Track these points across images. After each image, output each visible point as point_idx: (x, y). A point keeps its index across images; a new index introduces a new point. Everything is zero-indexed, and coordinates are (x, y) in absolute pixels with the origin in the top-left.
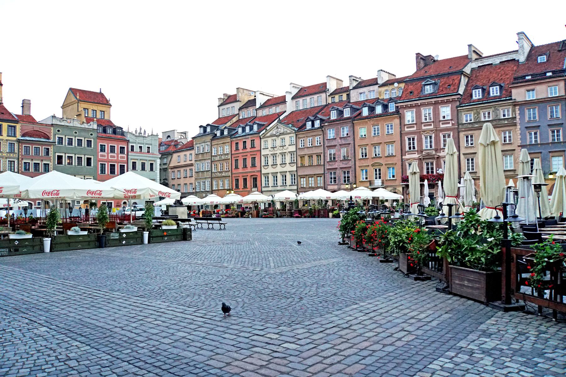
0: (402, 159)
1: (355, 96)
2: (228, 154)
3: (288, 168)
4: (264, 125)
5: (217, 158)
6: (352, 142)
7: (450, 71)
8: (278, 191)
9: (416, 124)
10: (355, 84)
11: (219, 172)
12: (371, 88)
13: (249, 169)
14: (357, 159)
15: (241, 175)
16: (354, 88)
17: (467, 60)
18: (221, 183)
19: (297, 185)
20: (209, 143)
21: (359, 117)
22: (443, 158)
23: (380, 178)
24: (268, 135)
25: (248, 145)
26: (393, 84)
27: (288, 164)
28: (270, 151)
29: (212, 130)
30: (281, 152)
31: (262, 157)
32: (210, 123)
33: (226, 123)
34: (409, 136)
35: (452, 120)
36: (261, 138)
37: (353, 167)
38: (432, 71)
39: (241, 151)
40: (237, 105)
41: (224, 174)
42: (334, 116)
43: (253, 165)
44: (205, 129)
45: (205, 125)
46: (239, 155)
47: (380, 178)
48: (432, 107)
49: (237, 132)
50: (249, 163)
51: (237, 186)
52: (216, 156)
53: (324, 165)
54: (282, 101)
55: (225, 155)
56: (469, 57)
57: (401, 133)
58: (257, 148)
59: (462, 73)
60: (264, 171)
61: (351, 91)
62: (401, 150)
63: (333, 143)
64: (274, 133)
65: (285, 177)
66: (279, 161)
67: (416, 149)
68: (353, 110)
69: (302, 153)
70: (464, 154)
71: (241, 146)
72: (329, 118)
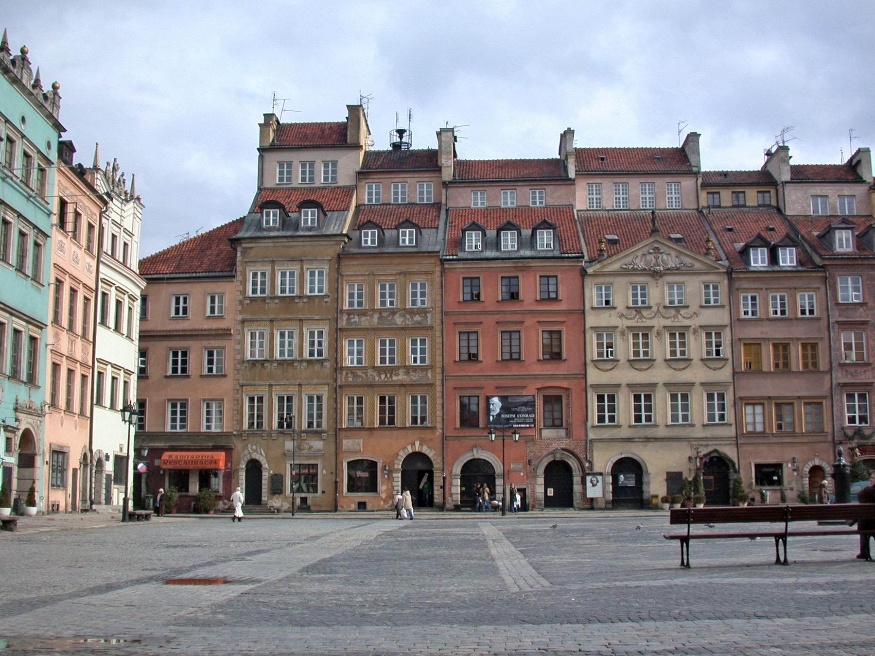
1: (799, 202)
2: (423, 312)
3: (697, 374)
5: (364, 322)
8: (656, 439)
28: (622, 316)
30: (668, 323)
41: (401, 377)
46: (482, 318)
52: (363, 313)
55: (412, 312)
60: (594, 376)
63: (859, 315)
64: (641, 265)
66: (661, 348)
69: (753, 332)
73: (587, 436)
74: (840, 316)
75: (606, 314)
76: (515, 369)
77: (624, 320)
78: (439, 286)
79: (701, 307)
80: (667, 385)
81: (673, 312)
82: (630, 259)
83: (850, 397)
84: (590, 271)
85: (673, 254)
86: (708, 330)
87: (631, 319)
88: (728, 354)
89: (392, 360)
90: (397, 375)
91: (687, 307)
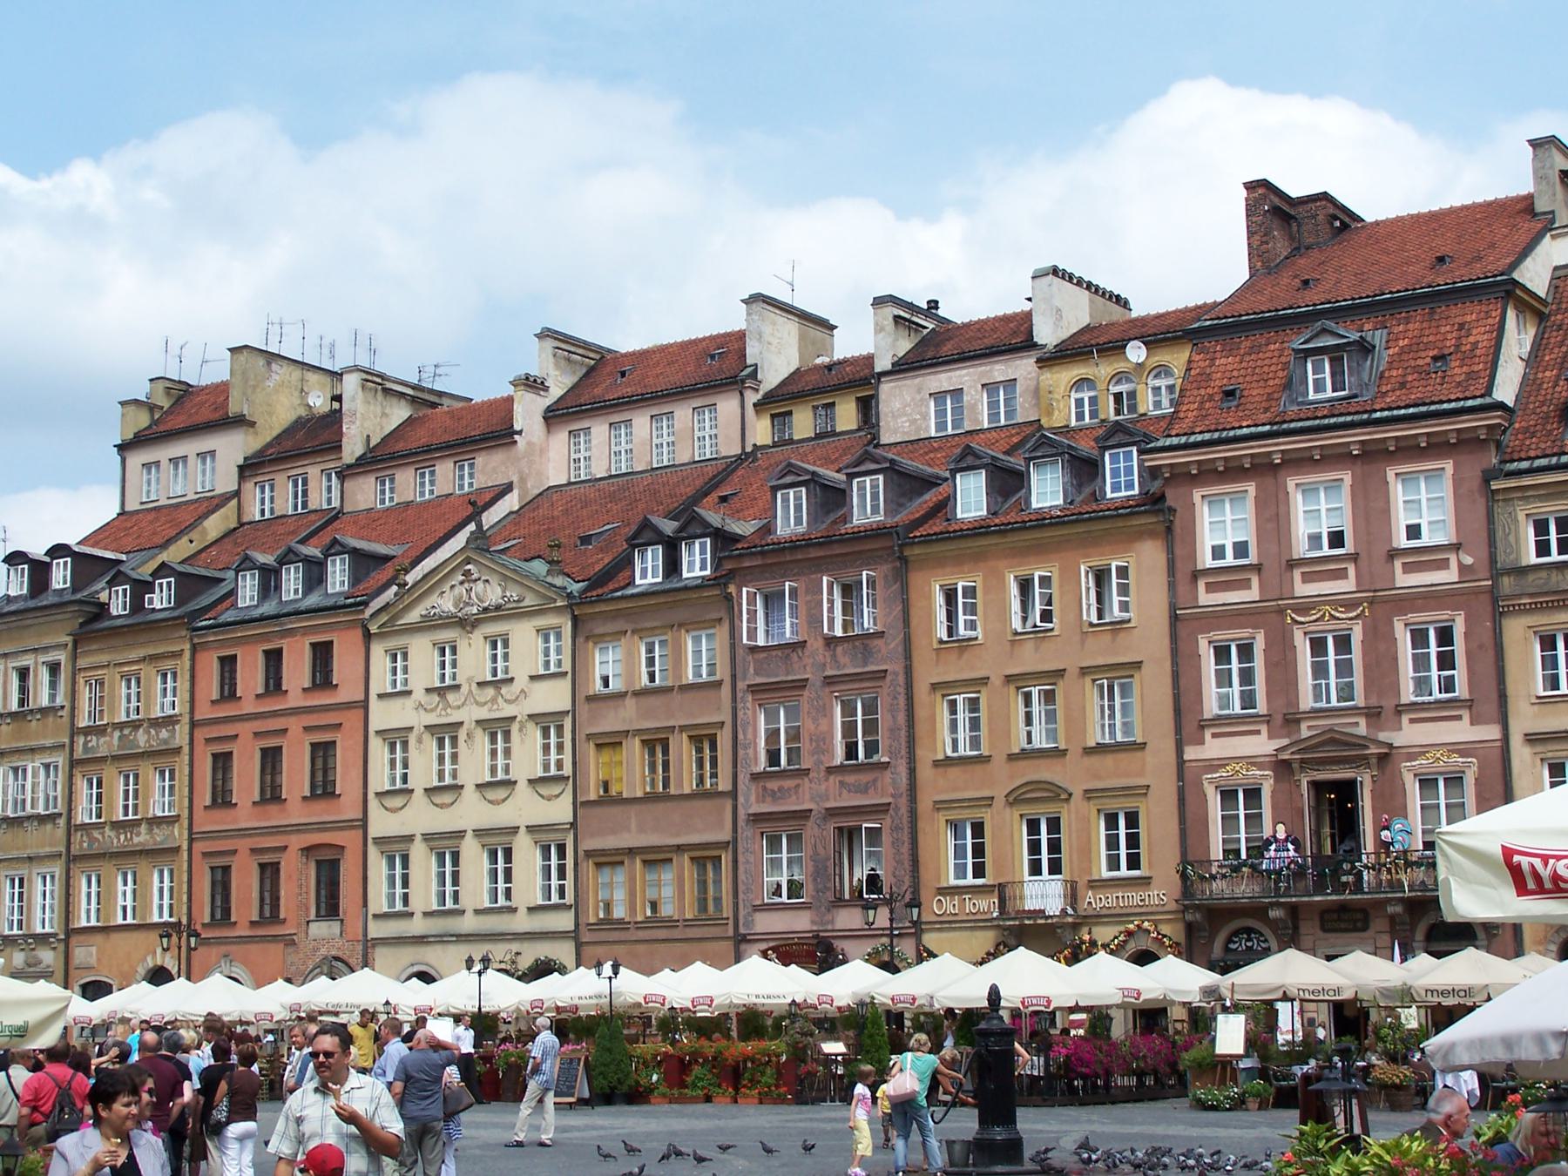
0: (1181, 763)
1: (908, 412)
2: (170, 721)
3: (525, 808)
4: (387, 559)
5: (106, 745)
6: (895, 667)
7: (1443, 279)
9: (1257, 568)
10: (905, 345)
11: (117, 825)
12: (999, 370)
13: (295, 811)
14: (924, 756)
15: (243, 845)
16: (904, 367)
17: (1528, 227)
18: (124, 893)
19: (577, 907)
20: (62, 656)
21: (937, 526)
22: (1412, 757)
23: (1055, 868)
24: (414, 616)
25: (297, 671)
26: (1115, 348)
27: (522, 786)
29: (78, 582)
30: (484, 714)
31: (376, 744)
32: (72, 539)
33: (164, 546)
34: (1220, 636)
35: (1456, 547)
36: (368, 636)
37: (903, 802)
38: (1340, 278)
39: (249, 707)
40: (231, 448)
41: (142, 838)
42: (791, 516)
43: (323, 788)
44: (39, 571)
45: (38, 550)
47: (1055, 868)
48: (1347, 477)
49: (232, 593)
50: (296, 774)
51: (222, 915)
52: (100, 731)
53: (733, 794)
54: (493, 429)
55: (156, 723)
56: (1541, 206)
57: (1174, 619)
58: (347, 691)
59: (1510, 292)
60: (382, 823)
61: (886, 388)
62: (1178, 711)
65: (508, 853)
67: (1262, 707)
68: (906, 482)
69: (611, 721)
70: (1532, 739)
71: (251, 676)
72: (768, 529)
73: (365, 935)
74: (757, 673)
75: (398, 703)
76: (274, 817)
77: (422, 712)
78: (187, 676)
79: (533, 678)
80: (479, 833)
81: (490, 691)
82: (433, 600)
83: (774, 844)
84: (374, 629)
85: (494, 580)
86: (545, 721)
87: (432, 710)
88: (567, 770)
89: (135, 813)
90: (138, 835)
91: (512, 679)
